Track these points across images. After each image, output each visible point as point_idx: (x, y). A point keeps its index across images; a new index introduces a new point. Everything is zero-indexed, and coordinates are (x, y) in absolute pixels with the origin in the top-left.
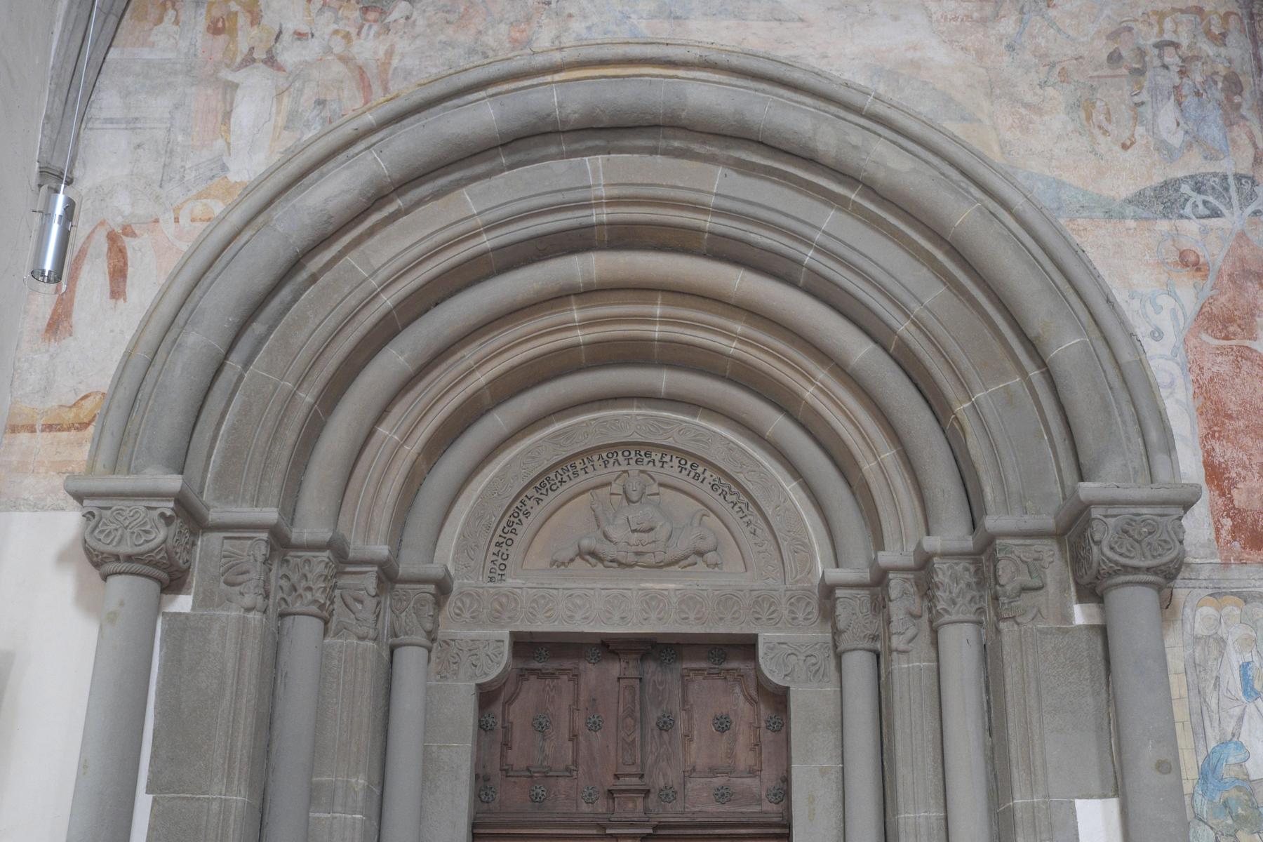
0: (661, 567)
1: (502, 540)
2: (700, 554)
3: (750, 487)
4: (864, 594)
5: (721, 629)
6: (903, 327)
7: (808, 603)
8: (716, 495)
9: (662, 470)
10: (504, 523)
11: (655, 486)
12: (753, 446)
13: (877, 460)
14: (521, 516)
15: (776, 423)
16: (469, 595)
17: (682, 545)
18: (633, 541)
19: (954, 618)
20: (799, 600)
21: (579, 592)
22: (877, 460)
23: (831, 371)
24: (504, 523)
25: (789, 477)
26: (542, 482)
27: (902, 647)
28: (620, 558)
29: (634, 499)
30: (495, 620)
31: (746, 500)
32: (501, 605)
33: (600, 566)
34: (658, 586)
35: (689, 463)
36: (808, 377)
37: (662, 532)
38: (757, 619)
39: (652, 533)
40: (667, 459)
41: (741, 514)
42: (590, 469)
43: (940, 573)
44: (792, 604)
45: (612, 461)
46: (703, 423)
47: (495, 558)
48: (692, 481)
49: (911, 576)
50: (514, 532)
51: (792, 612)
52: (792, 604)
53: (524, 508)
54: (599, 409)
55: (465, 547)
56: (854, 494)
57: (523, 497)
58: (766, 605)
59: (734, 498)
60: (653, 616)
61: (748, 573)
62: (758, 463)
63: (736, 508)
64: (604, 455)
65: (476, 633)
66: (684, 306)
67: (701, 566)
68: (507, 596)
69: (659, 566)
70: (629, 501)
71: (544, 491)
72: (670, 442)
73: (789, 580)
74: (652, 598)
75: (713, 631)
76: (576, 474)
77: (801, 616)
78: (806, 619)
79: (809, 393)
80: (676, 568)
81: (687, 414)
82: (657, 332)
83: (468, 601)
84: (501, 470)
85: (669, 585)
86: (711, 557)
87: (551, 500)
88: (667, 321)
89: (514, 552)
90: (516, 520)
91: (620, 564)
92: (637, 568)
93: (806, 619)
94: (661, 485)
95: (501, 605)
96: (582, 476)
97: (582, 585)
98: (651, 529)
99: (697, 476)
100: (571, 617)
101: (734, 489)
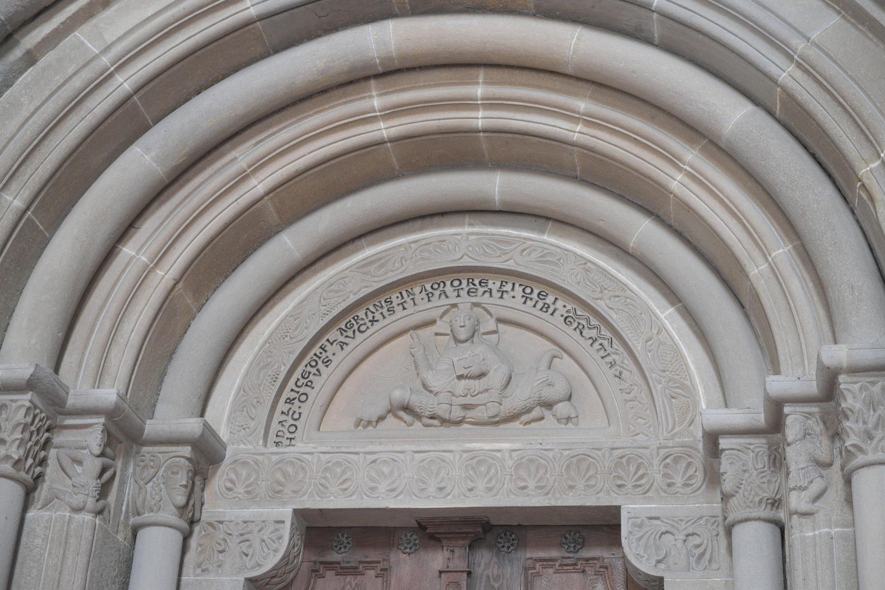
0: (497, 423)
2: (549, 405)
3: (614, 317)
4: (759, 443)
5: (571, 500)
6: (786, 74)
7: (689, 464)
8: (570, 330)
9: (501, 302)
12: (618, 265)
13: (767, 261)
14: (321, 366)
15: (641, 230)
16: (245, 463)
19: (871, 457)
21: (384, 456)
22: (767, 261)
23: (703, 150)
24: (297, 374)
25: (663, 302)
26: (347, 320)
27: (804, 507)
28: (440, 413)
30: (276, 494)
31: (609, 335)
33: (418, 424)
34: (487, 446)
35: (536, 292)
36: (673, 160)
37: (495, 379)
38: (620, 486)
39: (484, 380)
40: (508, 287)
41: (602, 353)
42: (409, 304)
43: (849, 397)
45: (437, 293)
46: (553, 240)
47: (284, 417)
48: (539, 313)
49: (814, 409)
53: (324, 355)
54: (421, 229)
56: (747, 316)
58: (632, 469)
59: (593, 333)
60: (481, 485)
62: (624, 287)
63: (596, 346)
64: (428, 287)
65: (250, 512)
66: (512, 84)
69: (497, 421)
70: (457, 341)
71: (350, 333)
72: (510, 265)
74: (480, 462)
75: (559, 503)
77: (679, 480)
78: (686, 485)
79: (676, 183)
80: (516, 424)
81: (532, 229)
82: (480, 119)
84: (294, 308)
85: (504, 444)
86: (562, 408)
87: (359, 344)
88: (492, 103)
89: (310, 411)
90: (314, 370)
92: (465, 426)
93: (686, 485)
94: (500, 320)
95: (285, 475)
96: (399, 313)
97: (390, 447)
98: (482, 375)
99: (545, 308)
100: (373, 489)
101: (594, 322)
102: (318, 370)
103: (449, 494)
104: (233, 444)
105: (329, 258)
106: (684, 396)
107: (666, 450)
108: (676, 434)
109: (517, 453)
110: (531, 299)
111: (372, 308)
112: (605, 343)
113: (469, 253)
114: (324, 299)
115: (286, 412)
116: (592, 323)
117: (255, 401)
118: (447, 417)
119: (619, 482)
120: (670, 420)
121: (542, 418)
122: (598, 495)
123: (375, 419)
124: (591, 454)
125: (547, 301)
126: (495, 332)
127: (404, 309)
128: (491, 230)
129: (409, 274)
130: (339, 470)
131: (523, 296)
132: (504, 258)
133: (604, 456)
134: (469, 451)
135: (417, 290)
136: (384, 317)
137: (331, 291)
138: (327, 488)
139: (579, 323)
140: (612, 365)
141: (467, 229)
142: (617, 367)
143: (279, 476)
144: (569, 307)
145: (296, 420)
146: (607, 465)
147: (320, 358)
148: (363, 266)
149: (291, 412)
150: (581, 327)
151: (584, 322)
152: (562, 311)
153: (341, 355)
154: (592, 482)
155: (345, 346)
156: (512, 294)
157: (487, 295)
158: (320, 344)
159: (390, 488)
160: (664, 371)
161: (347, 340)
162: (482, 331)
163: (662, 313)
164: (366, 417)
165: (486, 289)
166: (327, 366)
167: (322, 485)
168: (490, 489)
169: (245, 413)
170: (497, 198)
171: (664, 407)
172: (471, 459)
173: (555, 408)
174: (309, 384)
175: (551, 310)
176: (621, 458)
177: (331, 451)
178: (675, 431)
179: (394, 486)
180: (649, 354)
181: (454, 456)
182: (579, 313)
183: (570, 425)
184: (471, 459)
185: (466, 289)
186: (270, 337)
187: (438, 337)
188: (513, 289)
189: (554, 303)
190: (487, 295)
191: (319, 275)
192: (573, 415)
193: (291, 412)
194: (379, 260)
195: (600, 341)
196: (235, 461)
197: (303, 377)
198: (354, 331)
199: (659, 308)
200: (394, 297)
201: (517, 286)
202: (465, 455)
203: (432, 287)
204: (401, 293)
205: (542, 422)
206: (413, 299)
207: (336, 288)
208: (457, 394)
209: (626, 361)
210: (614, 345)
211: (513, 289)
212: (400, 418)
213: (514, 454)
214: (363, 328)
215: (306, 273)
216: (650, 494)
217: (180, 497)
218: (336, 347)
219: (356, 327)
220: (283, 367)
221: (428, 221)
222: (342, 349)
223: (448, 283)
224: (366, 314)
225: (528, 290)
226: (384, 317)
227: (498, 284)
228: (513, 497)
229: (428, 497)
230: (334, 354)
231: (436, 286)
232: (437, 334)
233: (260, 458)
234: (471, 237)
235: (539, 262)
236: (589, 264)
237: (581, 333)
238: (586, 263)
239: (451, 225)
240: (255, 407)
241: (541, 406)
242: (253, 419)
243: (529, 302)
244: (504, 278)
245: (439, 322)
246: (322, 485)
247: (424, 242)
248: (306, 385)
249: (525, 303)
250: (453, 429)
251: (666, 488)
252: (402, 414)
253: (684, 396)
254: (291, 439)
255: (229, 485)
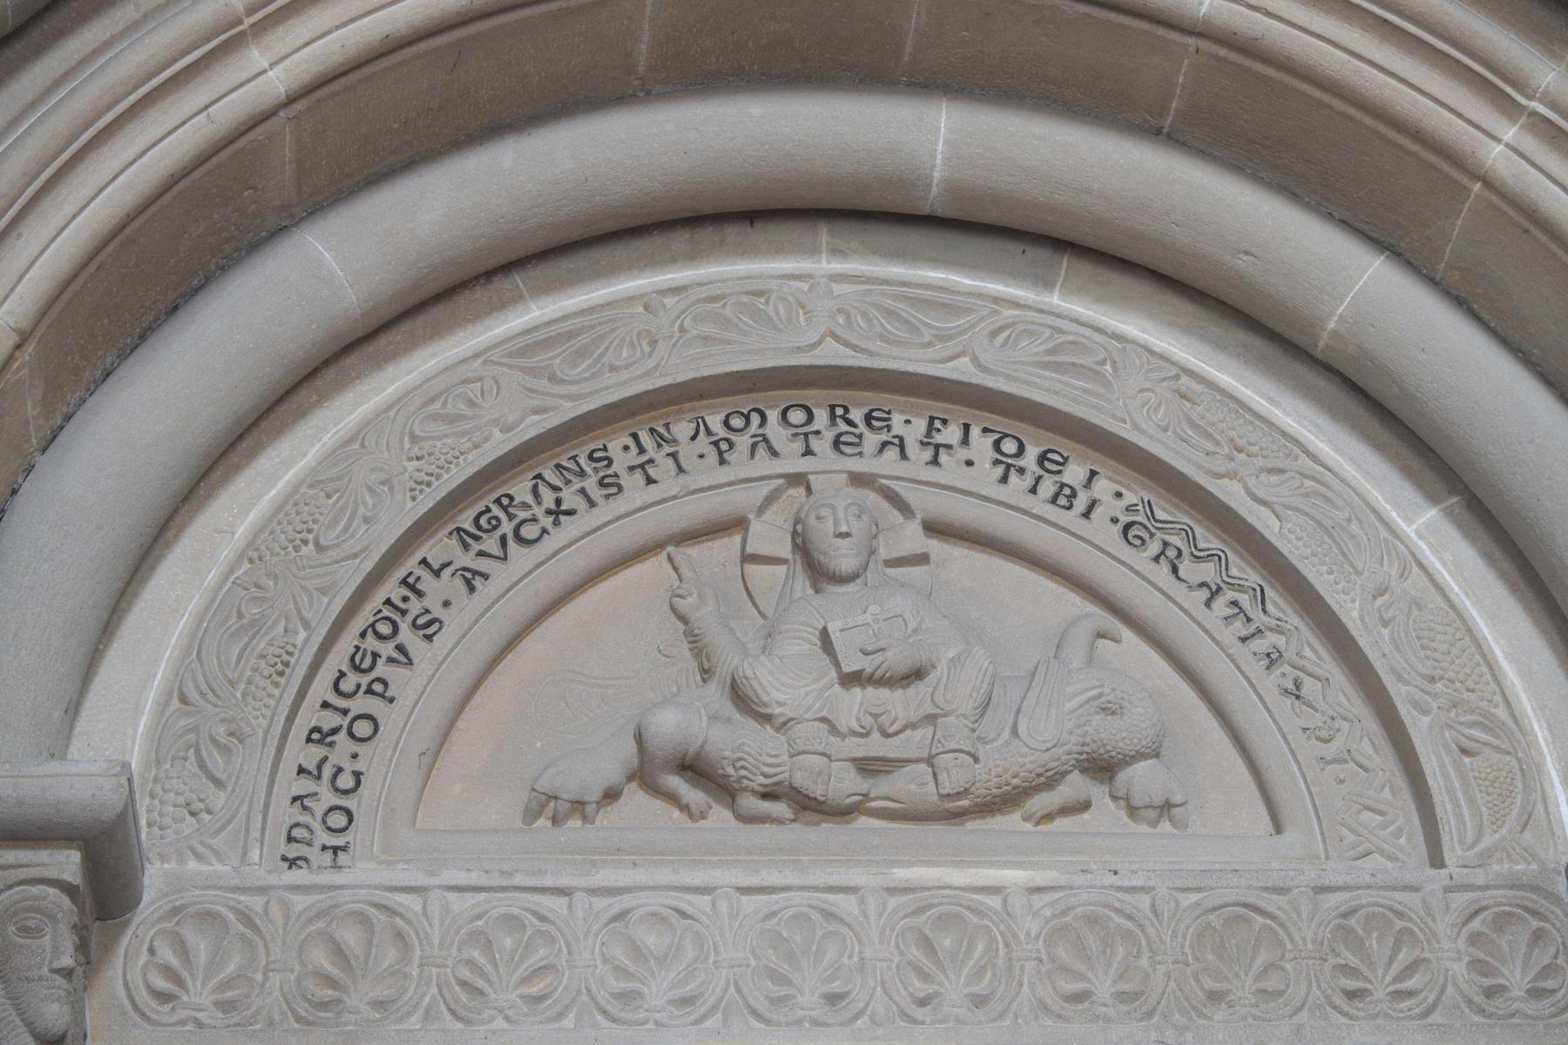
0: (957, 816)
1: (330, 720)
2: (1102, 767)
7: (1538, 935)
8: (1142, 559)
9: (932, 474)
10: (338, 658)
11: (914, 528)
12: (1269, 386)
14: (406, 635)
16: (208, 917)
17: (1047, 729)
18: (846, 721)
20: (1503, 921)
21: (654, 902)
24: (338, 658)
25: (1408, 492)
28: (801, 780)
29: (846, 565)
31: (1253, 578)
32: (339, 952)
33: (720, 815)
35: (1032, 452)
37: (956, 687)
38: (1352, 995)
39: (920, 689)
40: (951, 434)
41: (1239, 627)
42: (663, 468)
44: (1475, 939)
45: (743, 442)
46: (1078, 307)
47: (305, 786)
50: (379, 690)
51: (1478, 966)
52: (1475, 939)
53: (415, 606)
54: (693, 256)
55: (195, 719)
57: (411, 564)
59: (1208, 571)
61: (1290, 837)
63: (1220, 603)
64: (715, 422)
67: (1106, 812)
68: (363, 920)
69: (957, 810)
72: (961, 370)
73: (1453, 853)
76: (611, 485)
77: (1516, 979)
78: (1536, 993)
80: (1011, 821)
81: (1018, 276)
83: (201, 948)
86: (1142, 778)
87: (521, 577)
89: (384, 765)
90: (387, 649)
91: (809, 807)
92: (864, 821)
93: (1536, 993)
94: (934, 528)
95: (339, 952)
96: (635, 492)
97: (666, 876)
98: (917, 674)
99: (1064, 496)
101: (1207, 540)
102: (400, 648)
103: (861, 1013)
104: (163, 859)
105: (419, 321)
106: (1497, 749)
107: (1470, 895)
108: (1488, 853)
109: (1048, 897)
110: (1021, 471)
111: (548, 474)
112: (1244, 600)
113: (839, 331)
114: (414, 439)
115: (311, 767)
116: (1201, 545)
117: (222, 729)
118: (817, 792)
119: (1351, 984)
120: (1466, 812)
121: (1085, 806)
122: (1296, 1020)
123: (594, 795)
124: (1262, 904)
125: (1067, 478)
126: (923, 559)
127: (650, 481)
128: (897, 270)
129: (668, 381)
130: (508, 942)
131: (997, 462)
132: (951, 347)
133: (1297, 910)
134: (906, 890)
135: (682, 430)
136: (592, 503)
137: (434, 417)
138: (482, 993)
139: (1166, 544)
140: (1272, 660)
141: (826, 265)
142: (1286, 668)
143: (320, 958)
144: (1130, 498)
145: (346, 792)
146: (1310, 935)
147: (404, 613)
148: (523, 352)
149: (327, 771)
150: (1171, 553)
151: (1175, 540)
152: (1117, 509)
153: (467, 607)
154: (1272, 984)
155: (477, 582)
156: (963, 454)
157: (892, 453)
158: (401, 573)
159: (676, 994)
160: (1432, 679)
161: (483, 565)
162: (884, 553)
163: (1409, 521)
164: (570, 788)
165: (884, 437)
166: (429, 638)
167: (464, 984)
168: (979, 1001)
169: (192, 765)
170: (937, 175)
171: (1446, 776)
172: (915, 913)
173: (1122, 776)
174: (378, 687)
175: (1081, 503)
176: (1346, 915)
177: (485, 882)
178: (1483, 845)
179: (689, 988)
180: (1386, 632)
181: (862, 902)
182: (1160, 514)
183: (1166, 826)
184: (915, 913)
185: (829, 436)
186: (251, 543)
187: (751, 569)
188: (965, 441)
189: (1088, 485)
190: (892, 453)
191: (391, 370)
192: (1178, 799)
193: (327, 771)
194: (570, 335)
195: (1231, 595)
196: (175, 911)
197: (357, 668)
198: (503, 539)
199: (1397, 507)
200: (615, 449)
201: (975, 432)
202: (893, 902)
203: (726, 424)
204: (635, 436)
205: (1086, 816)
206: (673, 455)
207: (450, 409)
208: (843, 729)
209: (1307, 652)
210: (1270, 607)
211: (965, 441)
212: (672, 798)
213: (1039, 900)
214: (529, 532)
215: (349, 361)
216: (1436, 1018)
217: (55, 1007)
218: (449, 585)
219: (507, 528)
220: (302, 635)
221: (707, 234)
222: (472, 589)
223: (773, 416)
224: (535, 491)
225: (1009, 446)
226: (592, 503)
227: (920, 425)
228: (1049, 1022)
229: (798, 1022)
230: (446, 604)
231: (737, 422)
232: (747, 558)
233: (256, 903)
234: (838, 288)
235: (1046, 366)
236: (1185, 380)
237: (1175, 570)
238: (1177, 377)
239: (778, 251)
240: (224, 750)
241: (1083, 771)
242: (219, 784)
243: (1013, 477)
244: (938, 408)
245: (755, 526)
246: (464, 984)
247: (704, 293)
248: (370, 691)
249: (1004, 479)
250: (827, 832)
251: (1480, 999)
252: (675, 782)
253: (1497, 749)
254: (336, 850)
255: (160, 983)
